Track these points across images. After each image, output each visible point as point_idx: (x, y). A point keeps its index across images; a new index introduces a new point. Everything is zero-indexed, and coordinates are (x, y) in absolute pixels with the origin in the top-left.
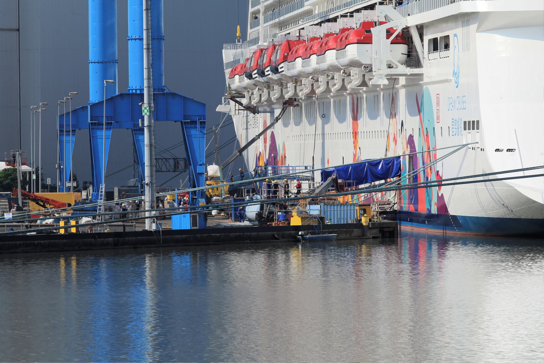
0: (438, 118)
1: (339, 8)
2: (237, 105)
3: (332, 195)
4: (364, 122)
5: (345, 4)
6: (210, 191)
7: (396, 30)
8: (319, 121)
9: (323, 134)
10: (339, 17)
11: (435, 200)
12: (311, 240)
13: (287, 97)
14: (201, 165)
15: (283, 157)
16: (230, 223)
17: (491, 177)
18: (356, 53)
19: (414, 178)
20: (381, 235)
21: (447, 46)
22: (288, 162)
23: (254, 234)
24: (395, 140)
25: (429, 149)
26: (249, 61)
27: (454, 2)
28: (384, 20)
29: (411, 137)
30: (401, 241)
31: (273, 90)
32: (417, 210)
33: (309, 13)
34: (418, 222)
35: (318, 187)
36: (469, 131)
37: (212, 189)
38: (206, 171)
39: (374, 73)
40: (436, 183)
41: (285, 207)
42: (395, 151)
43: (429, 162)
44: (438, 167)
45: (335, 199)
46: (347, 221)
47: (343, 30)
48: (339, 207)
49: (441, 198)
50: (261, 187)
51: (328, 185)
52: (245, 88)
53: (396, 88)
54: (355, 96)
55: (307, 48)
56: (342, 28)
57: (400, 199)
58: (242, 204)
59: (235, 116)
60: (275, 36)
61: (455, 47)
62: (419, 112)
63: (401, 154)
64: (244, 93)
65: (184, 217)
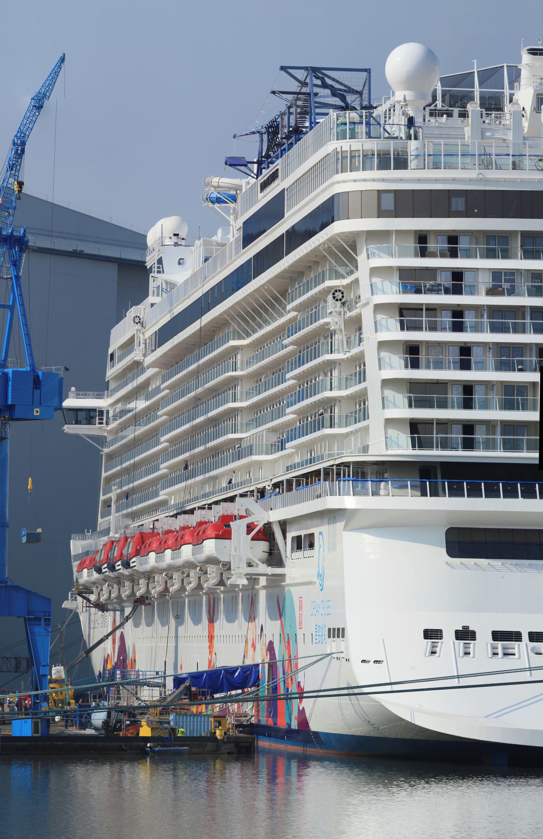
0: (301, 623)
1: (196, 499)
2: (85, 601)
3: (185, 704)
4: (222, 625)
5: (203, 495)
6: (54, 695)
7: (257, 526)
8: (172, 622)
9: (177, 637)
10: (197, 509)
11: (295, 714)
12: (160, 753)
13: (138, 594)
14: (44, 666)
15: (133, 660)
16: (74, 731)
17: (356, 691)
18: (214, 549)
19: (273, 689)
20: (236, 750)
21: (311, 546)
22: (138, 666)
23: (100, 744)
24: (254, 646)
25: (290, 657)
26: (99, 554)
27: (320, 496)
28: (244, 514)
29: (271, 643)
30: (258, 757)
31: (124, 586)
32: (275, 724)
33: (164, 504)
34: (276, 737)
35: (170, 695)
36: (334, 639)
37: (56, 693)
38: (50, 674)
39: (232, 572)
40: (297, 696)
41: (134, 716)
42: (253, 659)
43: (290, 672)
44: (300, 677)
45: (188, 709)
46: (200, 734)
47: (200, 524)
48: (192, 717)
49: (302, 712)
50: (108, 692)
51: (180, 694)
52: (94, 583)
53: (255, 589)
54: (212, 596)
55: (161, 541)
56: (199, 520)
57: (258, 711)
58: (87, 711)
59: (82, 614)
60: (126, 527)
61: (320, 546)
62: (281, 616)
63: (260, 662)
64: (92, 589)
65: (25, 722)
